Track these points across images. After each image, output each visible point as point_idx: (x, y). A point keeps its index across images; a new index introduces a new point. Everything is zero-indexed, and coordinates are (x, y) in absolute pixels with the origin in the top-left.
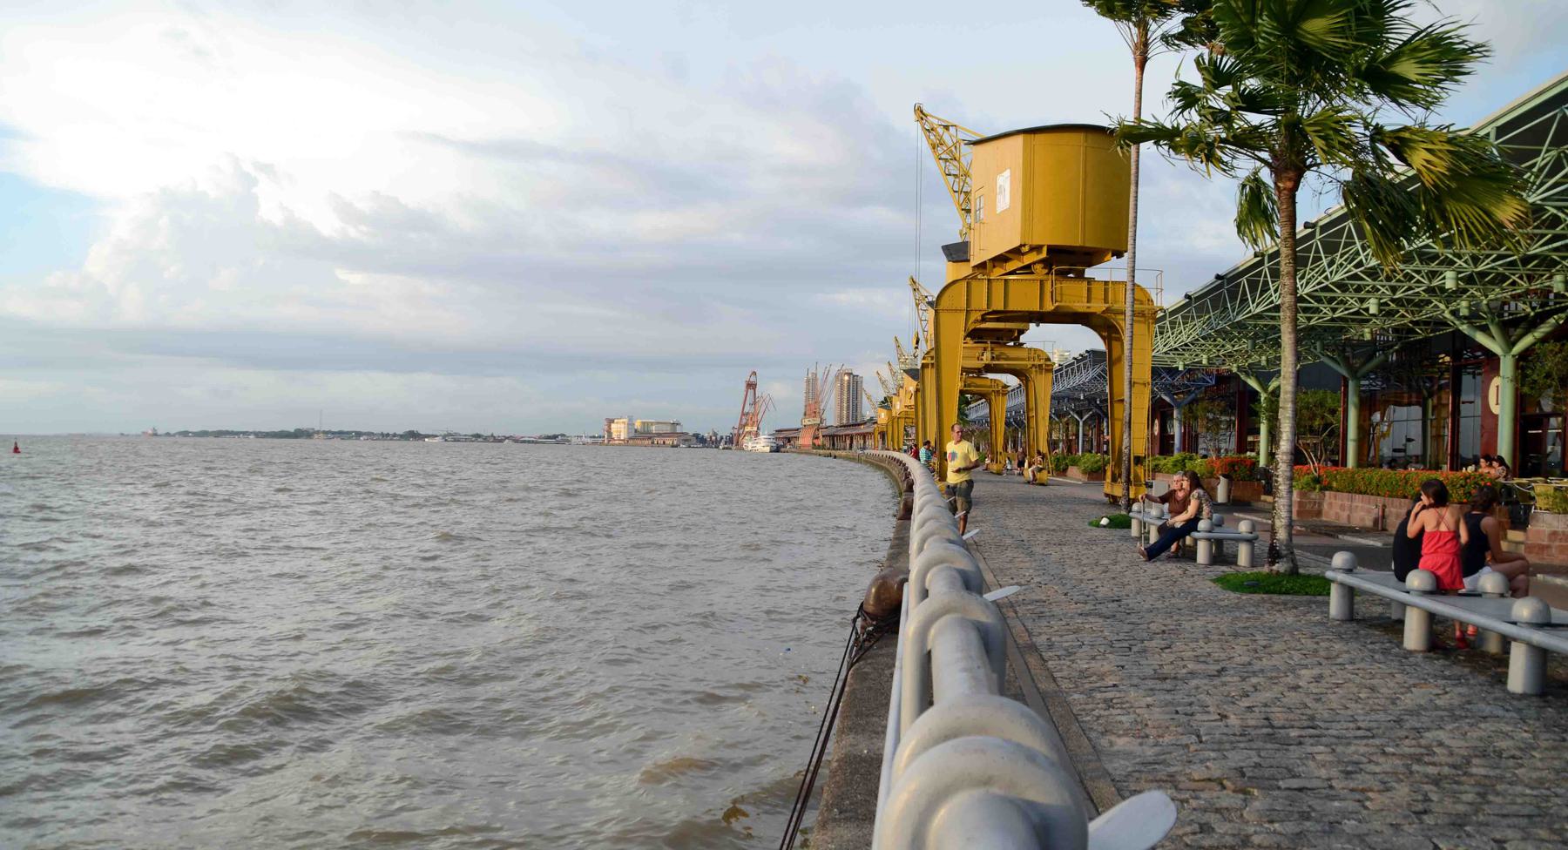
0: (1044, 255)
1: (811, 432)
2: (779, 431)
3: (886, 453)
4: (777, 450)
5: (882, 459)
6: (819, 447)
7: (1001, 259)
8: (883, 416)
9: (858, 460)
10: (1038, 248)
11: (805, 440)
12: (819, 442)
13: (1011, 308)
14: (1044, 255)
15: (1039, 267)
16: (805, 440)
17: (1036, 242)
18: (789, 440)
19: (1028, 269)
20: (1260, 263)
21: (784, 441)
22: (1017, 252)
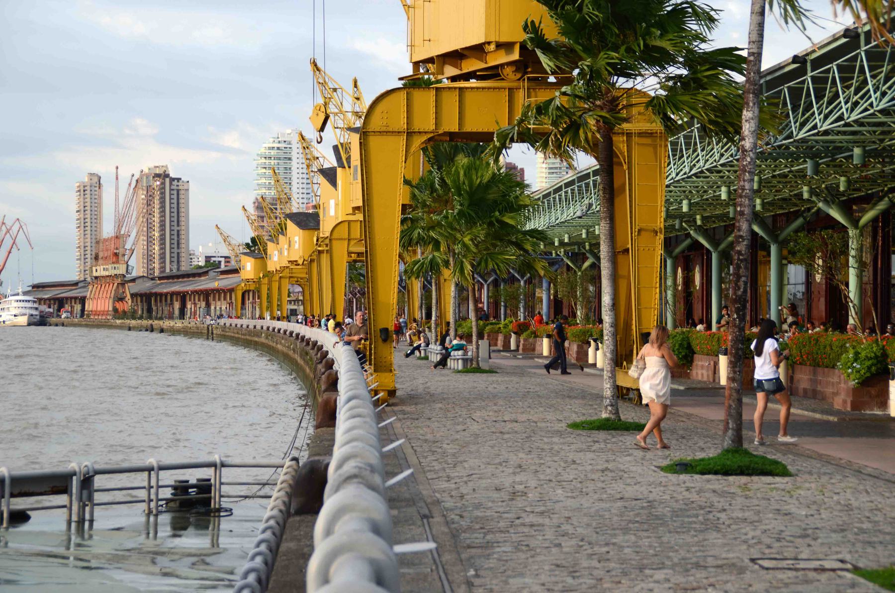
0: (516, 56)
1: (110, 290)
2: (37, 287)
3: (259, 323)
4: (41, 321)
5: (255, 332)
6: (124, 315)
7: (455, 57)
8: (249, 267)
9: (208, 334)
10: (506, 46)
11: (100, 302)
12: (128, 305)
13: (469, 127)
14: (516, 56)
15: (508, 70)
16: (100, 302)
17: (504, 39)
18: (60, 303)
19: (493, 73)
20: (800, 72)
21: (55, 304)
22: (478, 50)
